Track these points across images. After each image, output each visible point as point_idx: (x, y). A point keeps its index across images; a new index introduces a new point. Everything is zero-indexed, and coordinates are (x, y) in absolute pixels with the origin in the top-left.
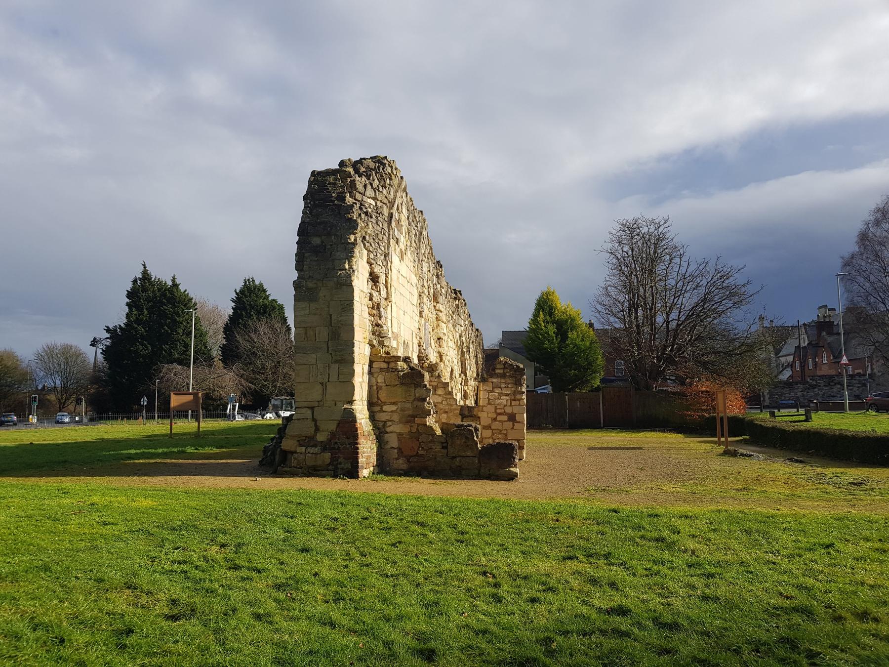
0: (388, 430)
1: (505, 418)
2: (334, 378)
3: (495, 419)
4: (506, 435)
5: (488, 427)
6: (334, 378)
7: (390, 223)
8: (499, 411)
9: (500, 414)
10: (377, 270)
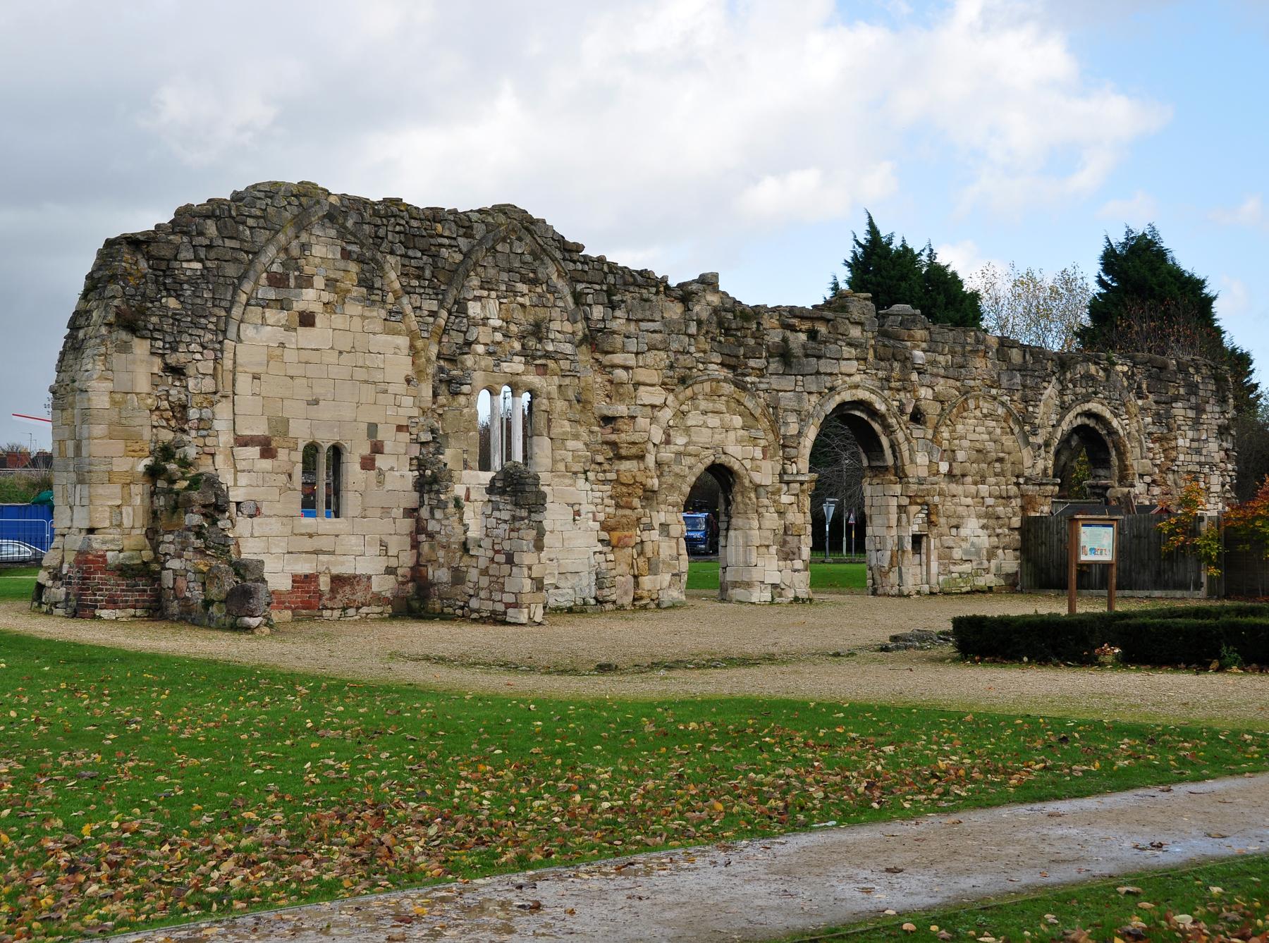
0: (168, 565)
1: (501, 558)
2: (77, 503)
3: (492, 560)
4: (503, 584)
5: (485, 572)
6: (77, 503)
7: (240, 284)
8: (497, 547)
9: (497, 552)
10: (172, 359)
